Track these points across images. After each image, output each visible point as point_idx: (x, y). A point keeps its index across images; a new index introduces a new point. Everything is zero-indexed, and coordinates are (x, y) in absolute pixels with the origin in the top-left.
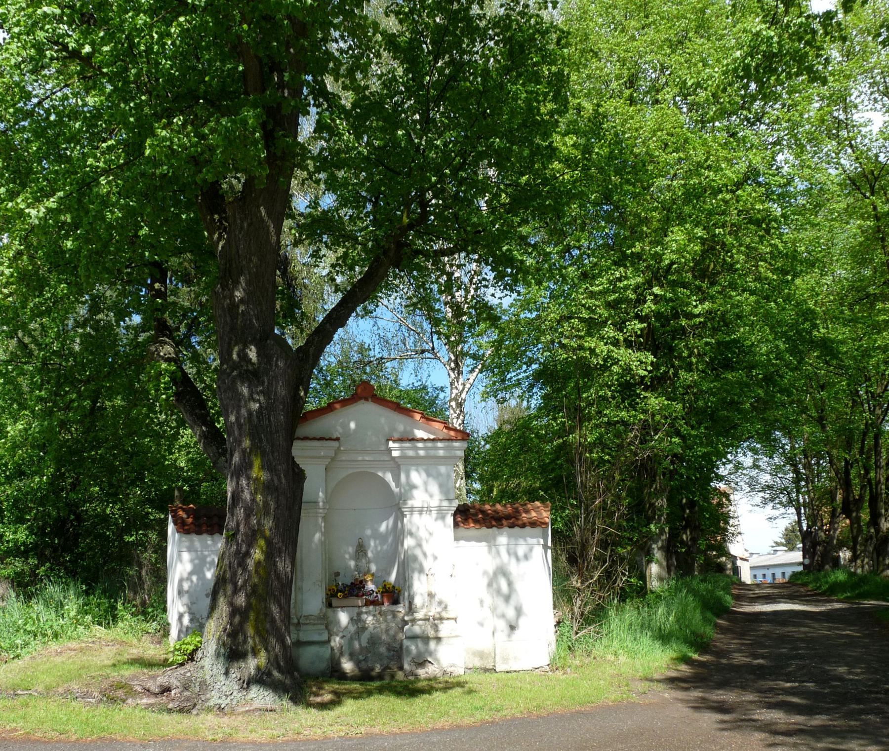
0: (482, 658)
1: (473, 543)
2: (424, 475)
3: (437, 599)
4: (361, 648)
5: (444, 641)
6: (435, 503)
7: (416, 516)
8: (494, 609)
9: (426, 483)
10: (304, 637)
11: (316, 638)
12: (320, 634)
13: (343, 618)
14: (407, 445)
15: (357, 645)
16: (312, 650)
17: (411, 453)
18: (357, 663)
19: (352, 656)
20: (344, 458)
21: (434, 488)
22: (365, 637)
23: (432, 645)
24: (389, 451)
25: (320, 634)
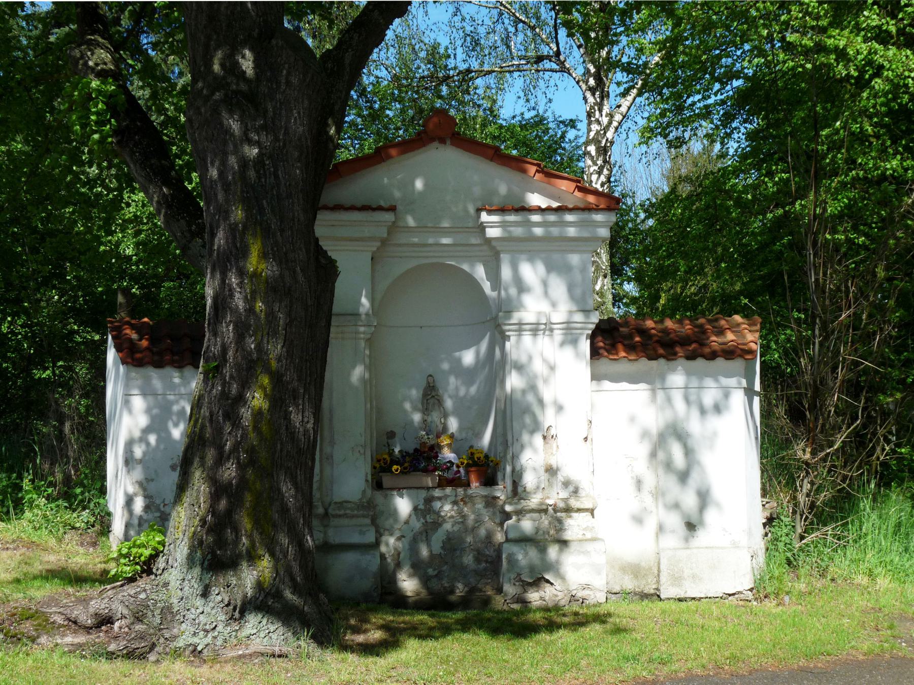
0: (636, 577)
1: (625, 385)
2: (541, 268)
3: (560, 477)
4: (432, 556)
5: (573, 547)
6: (559, 316)
7: (527, 338)
8: (659, 493)
9: (545, 284)
10: (335, 537)
11: (356, 539)
12: (362, 533)
13: (403, 505)
14: (512, 218)
15: (424, 552)
16: (350, 558)
17: (518, 231)
18: (425, 581)
19: (418, 568)
20: (403, 241)
21: (559, 288)
22: (438, 538)
23: (553, 552)
24: (482, 228)
25: (362, 533)
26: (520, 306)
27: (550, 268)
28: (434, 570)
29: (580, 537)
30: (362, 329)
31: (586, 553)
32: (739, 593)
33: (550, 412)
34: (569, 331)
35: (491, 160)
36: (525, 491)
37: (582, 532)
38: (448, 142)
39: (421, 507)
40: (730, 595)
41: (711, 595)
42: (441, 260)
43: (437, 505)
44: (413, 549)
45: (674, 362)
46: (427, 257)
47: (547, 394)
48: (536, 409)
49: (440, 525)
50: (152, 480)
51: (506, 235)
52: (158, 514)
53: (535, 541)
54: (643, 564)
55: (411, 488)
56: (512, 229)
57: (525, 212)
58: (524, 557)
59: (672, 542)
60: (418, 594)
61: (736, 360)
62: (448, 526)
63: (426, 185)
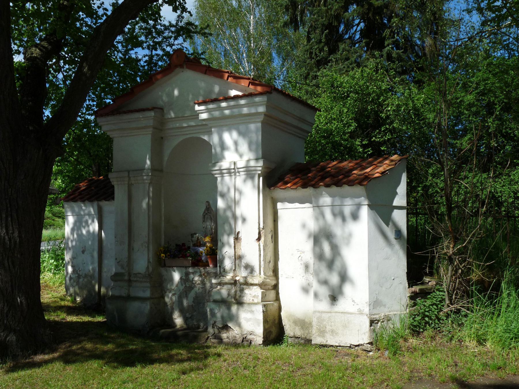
0: (302, 328)
1: (297, 205)
2: (235, 134)
3: (244, 262)
4: (189, 306)
5: (246, 307)
6: (241, 164)
7: (227, 178)
8: (316, 273)
9: (236, 143)
10: (133, 294)
11: (141, 294)
12: (144, 291)
13: (177, 276)
14: (211, 106)
15: (185, 303)
16: (136, 305)
17: (217, 114)
18: (186, 320)
19: (183, 312)
20: (171, 126)
21: (244, 147)
22: (192, 294)
23: (234, 308)
24: (196, 114)
25: (144, 291)
26: (221, 158)
27: (241, 133)
28: (190, 314)
29: (251, 301)
30: (145, 177)
31: (252, 312)
32: (361, 345)
33: (239, 222)
34: (249, 173)
35: (205, 73)
36: (224, 271)
37: (252, 299)
38: (185, 67)
39: (184, 278)
40: (356, 346)
41: (343, 345)
42: (195, 135)
43: (191, 276)
44: (180, 302)
45: (319, 189)
46: (187, 134)
47: (238, 212)
48: (232, 222)
49: (193, 288)
50: (75, 258)
51: (211, 117)
52: (77, 275)
53: (224, 302)
54: (306, 320)
55: (180, 267)
56: (213, 113)
57: (218, 102)
58: (220, 312)
59: (324, 305)
60: (182, 327)
61: (308, 188)
62: (196, 289)
63: (180, 92)
